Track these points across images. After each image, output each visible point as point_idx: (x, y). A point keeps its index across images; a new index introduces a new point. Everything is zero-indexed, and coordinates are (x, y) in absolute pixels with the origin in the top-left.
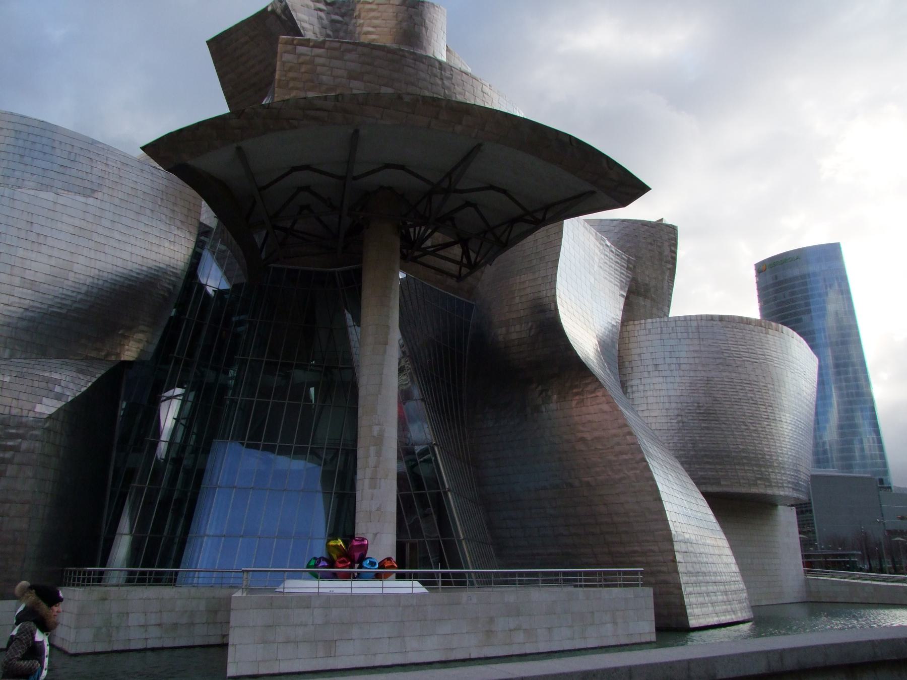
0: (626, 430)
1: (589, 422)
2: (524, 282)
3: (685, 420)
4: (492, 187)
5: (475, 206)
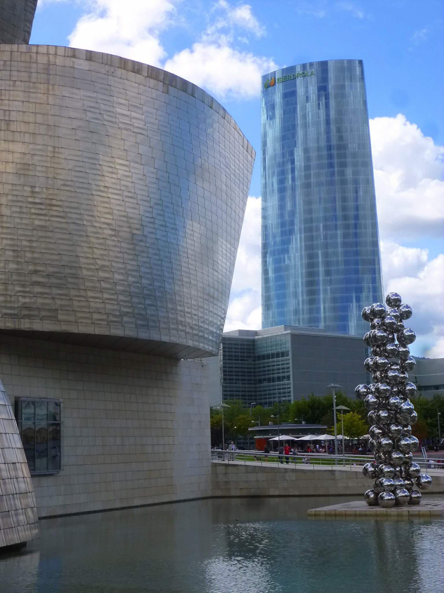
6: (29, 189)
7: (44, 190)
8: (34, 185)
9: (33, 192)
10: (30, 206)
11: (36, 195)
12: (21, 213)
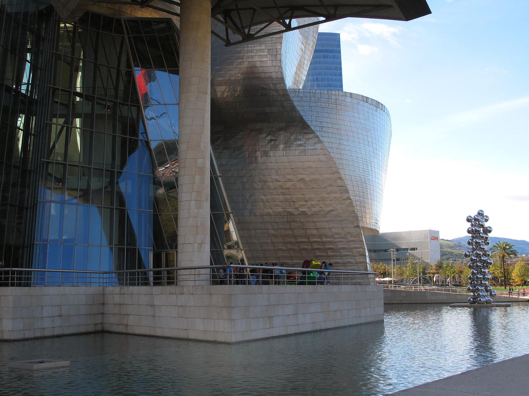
0: (336, 175)
1: (310, 167)
2: (251, 51)
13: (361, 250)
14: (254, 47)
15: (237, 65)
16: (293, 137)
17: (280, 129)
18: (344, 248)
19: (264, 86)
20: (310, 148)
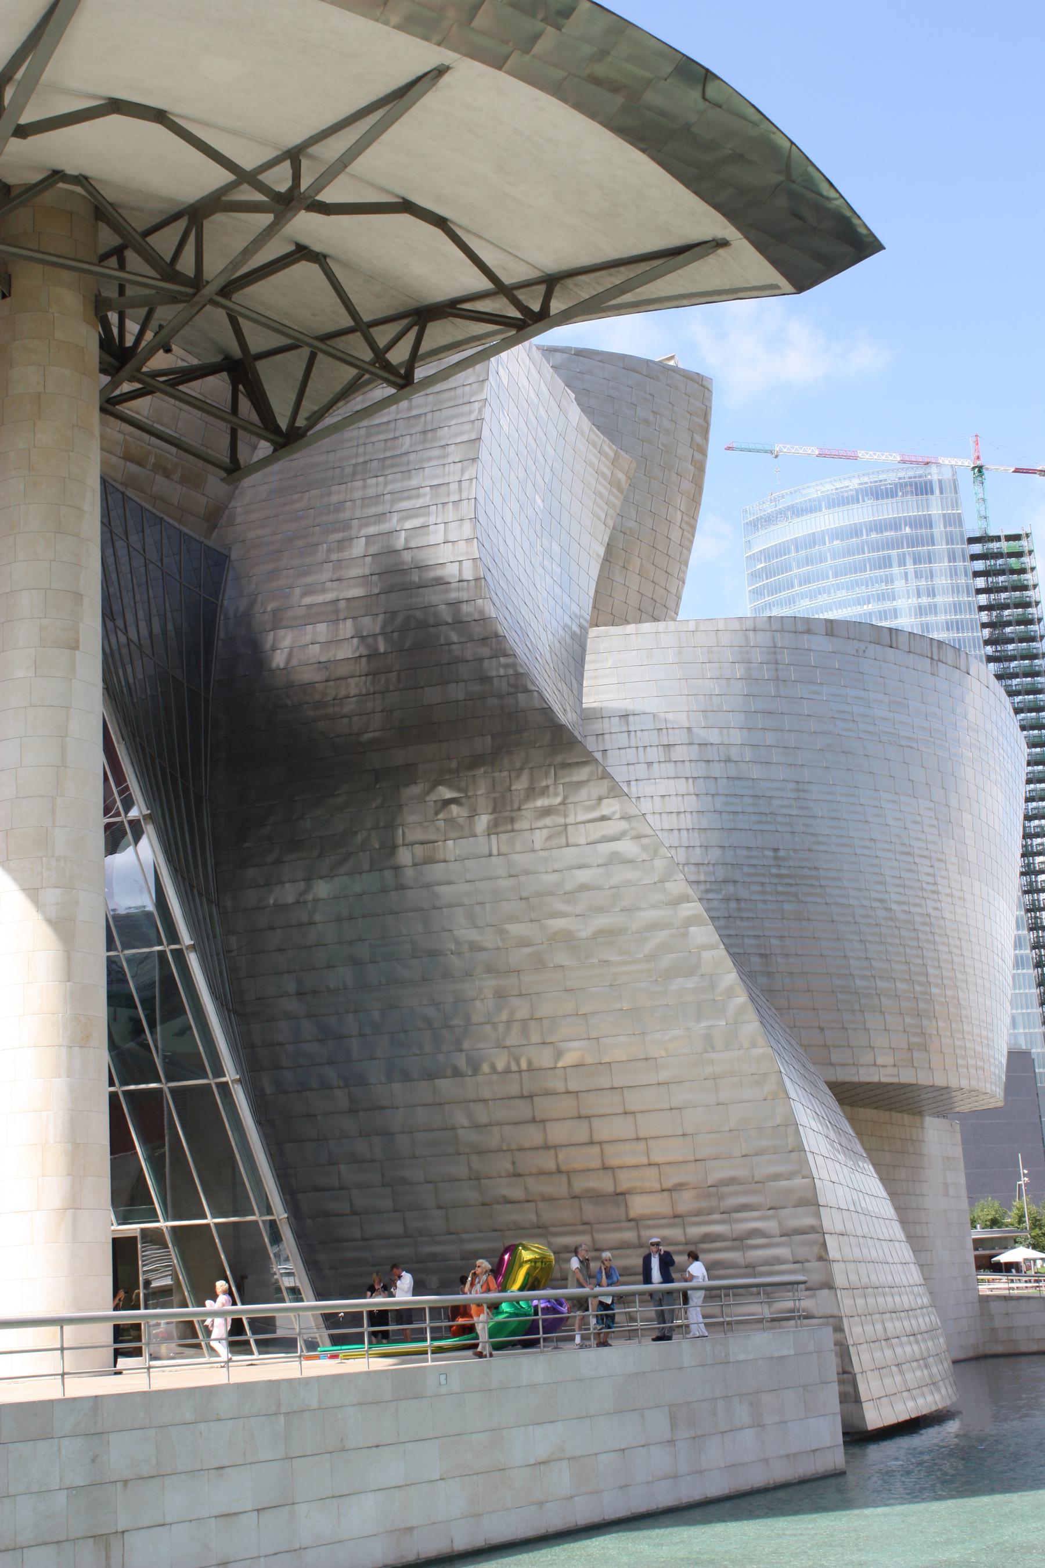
1: (584, 888)
2: (378, 498)
3: (744, 893)
4: (406, 207)
5: (319, 258)
6: (770, 853)
7: (791, 853)
8: (775, 846)
9: (776, 858)
10: (775, 881)
11: (781, 863)
12: (763, 893)
13: (798, 1182)
14: (386, 484)
15: (329, 551)
16: (521, 785)
17: (475, 762)
18: (732, 1181)
19: (419, 614)
20: (581, 817)
